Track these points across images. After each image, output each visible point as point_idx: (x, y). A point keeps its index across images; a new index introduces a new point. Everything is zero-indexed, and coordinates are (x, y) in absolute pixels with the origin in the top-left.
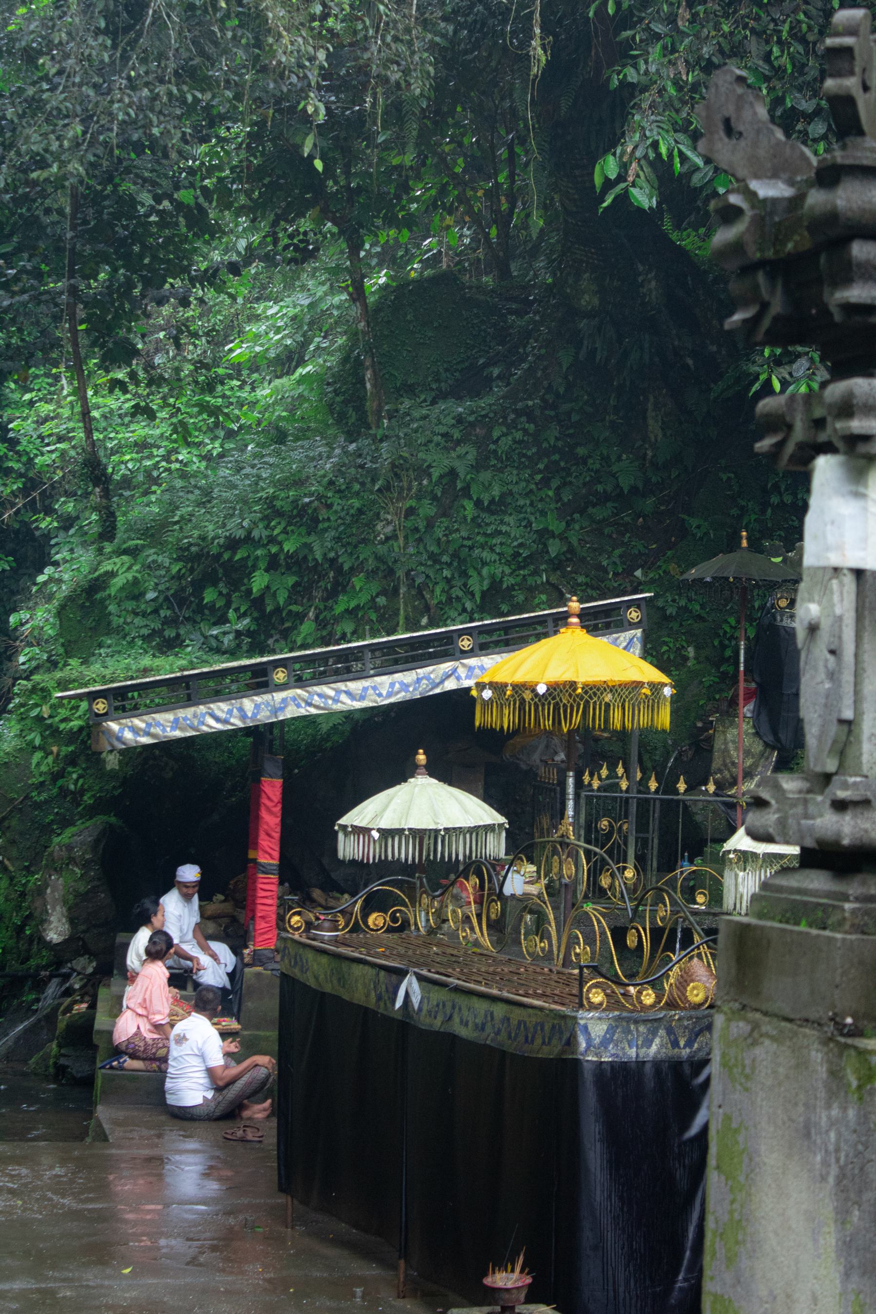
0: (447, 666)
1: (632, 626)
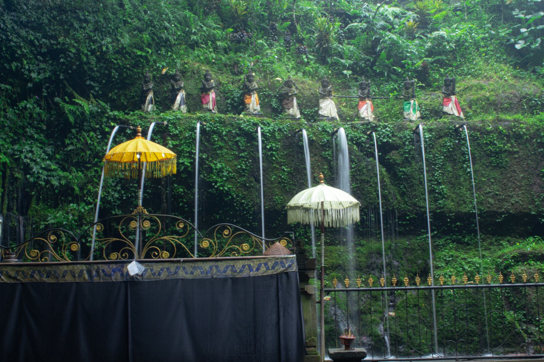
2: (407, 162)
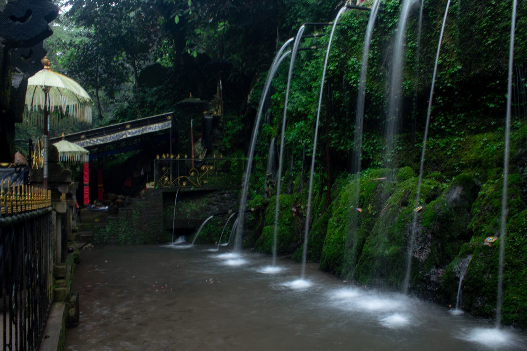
0: (124, 132)
1: (169, 120)
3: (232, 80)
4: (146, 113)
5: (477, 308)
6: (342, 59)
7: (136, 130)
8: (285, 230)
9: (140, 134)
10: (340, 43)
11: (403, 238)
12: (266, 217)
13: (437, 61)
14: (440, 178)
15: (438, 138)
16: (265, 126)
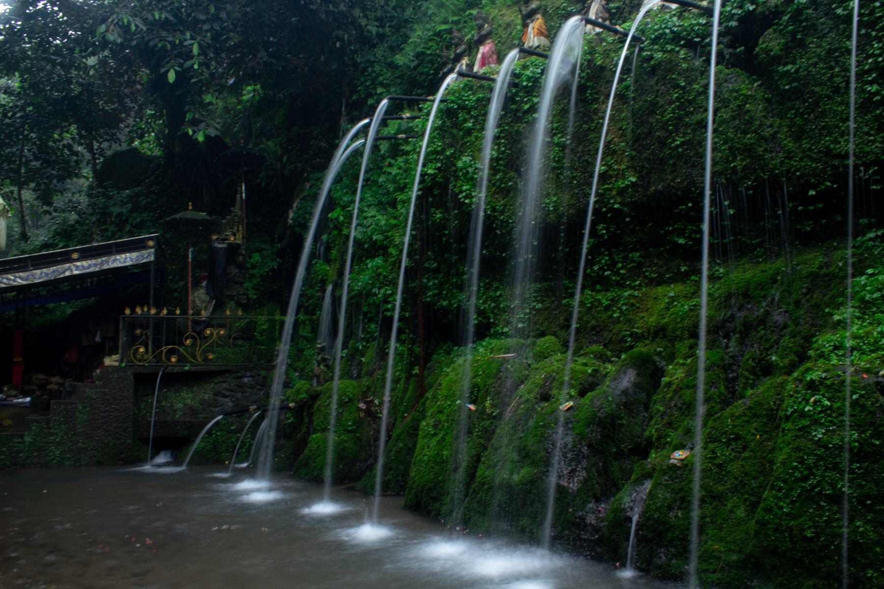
0: (67, 265)
1: (151, 248)
2: (795, 45)
3: (263, 185)
4: (110, 234)
5: (660, 567)
6: (448, 157)
7: (89, 262)
8: (345, 441)
9: (97, 269)
10: (446, 131)
11: (543, 453)
12: (315, 418)
13: (598, 168)
14: (601, 355)
15: (599, 291)
16: (316, 263)
